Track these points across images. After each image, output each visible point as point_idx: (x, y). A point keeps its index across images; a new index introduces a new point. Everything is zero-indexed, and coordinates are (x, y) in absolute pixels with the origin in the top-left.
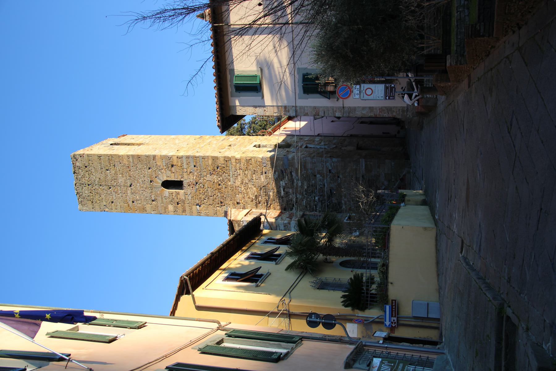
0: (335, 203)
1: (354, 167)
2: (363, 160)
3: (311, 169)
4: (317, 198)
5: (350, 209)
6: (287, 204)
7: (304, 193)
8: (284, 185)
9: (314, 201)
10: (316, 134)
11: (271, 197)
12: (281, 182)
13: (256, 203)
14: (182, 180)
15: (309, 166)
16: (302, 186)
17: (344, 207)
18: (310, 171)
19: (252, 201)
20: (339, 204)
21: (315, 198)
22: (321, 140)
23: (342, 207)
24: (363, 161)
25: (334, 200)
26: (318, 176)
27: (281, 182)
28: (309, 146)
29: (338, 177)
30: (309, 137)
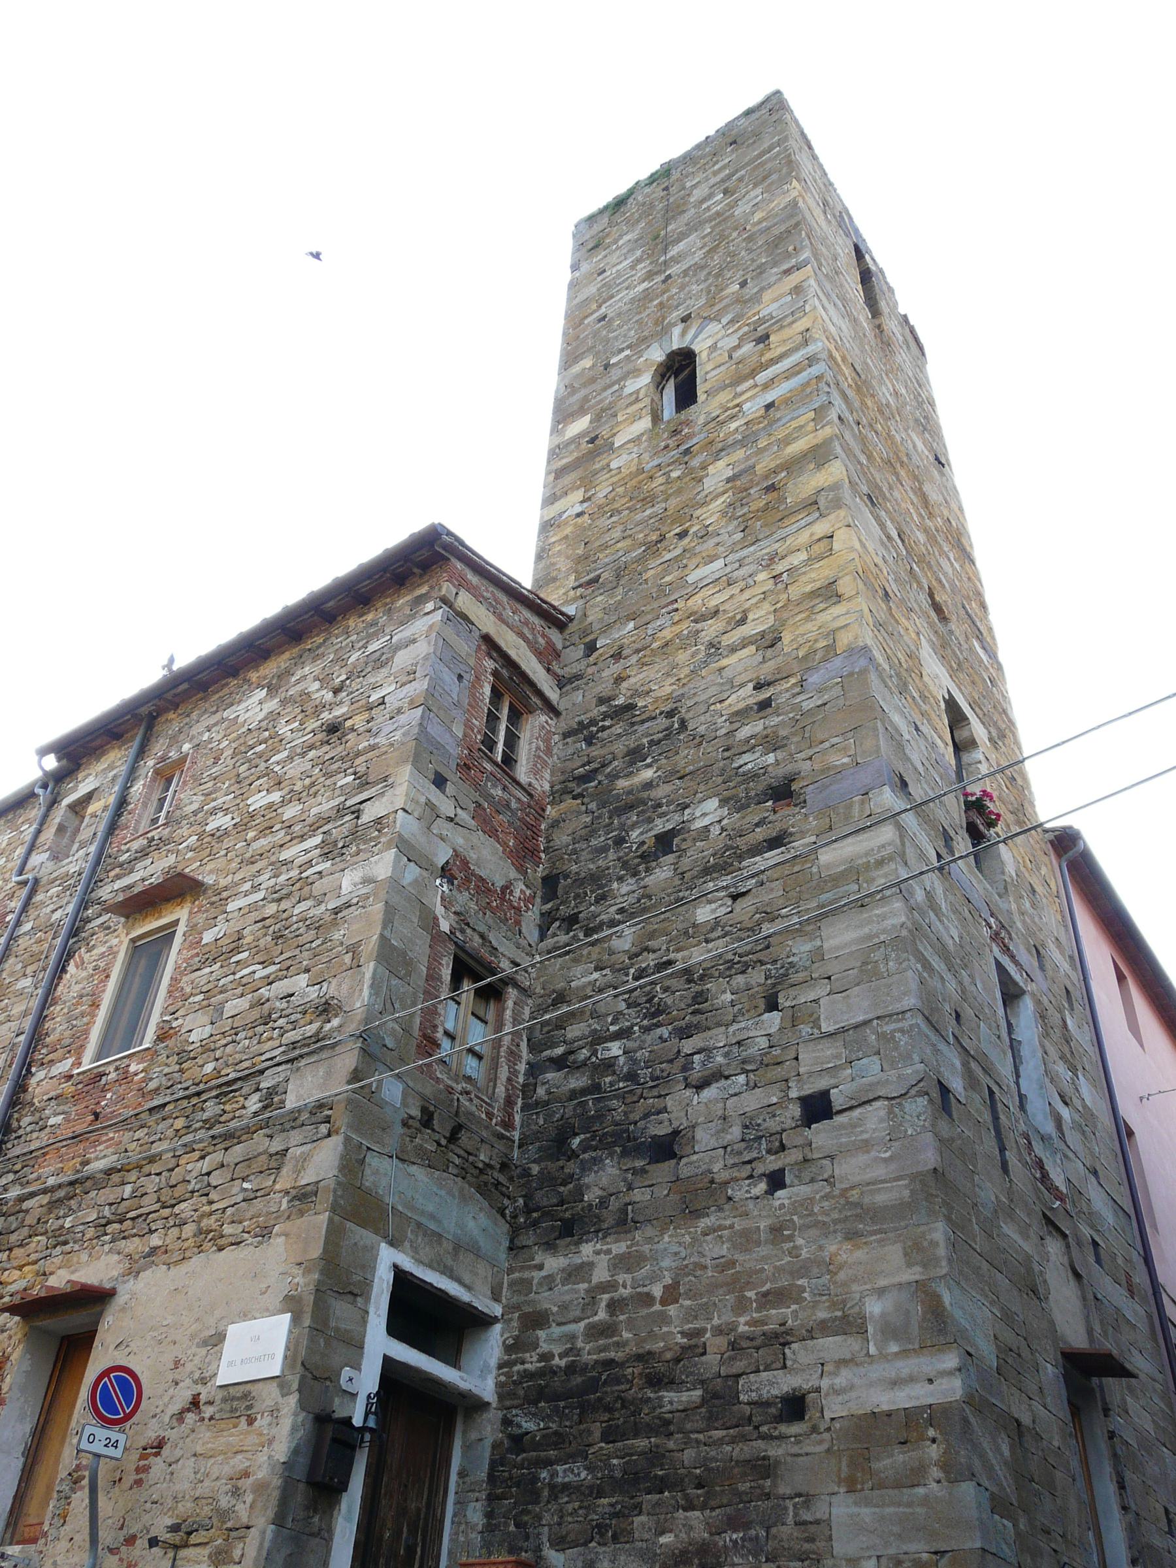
0: (579, 1193)
1: (874, 1308)
2: (951, 1389)
3: (818, 955)
4: (615, 1049)
5: (536, 1320)
6: (579, 882)
7: (649, 960)
8: (699, 824)
9: (598, 1039)
10: (1129, 1111)
11: (622, 783)
12: (713, 803)
13: (594, 722)
14: (701, 397)
15: (841, 937)
16: (693, 933)
17: (553, 1263)
18: (801, 948)
19: (602, 701)
20: (571, 1228)
21: (617, 1036)
22: (1088, 1115)
23: (550, 1246)
24: (937, 1381)
25: (604, 1178)
26: (773, 1020)
27: (713, 803)
28: (1027, 1006)
29: (776, 1181)
30: (1093, 1051)
